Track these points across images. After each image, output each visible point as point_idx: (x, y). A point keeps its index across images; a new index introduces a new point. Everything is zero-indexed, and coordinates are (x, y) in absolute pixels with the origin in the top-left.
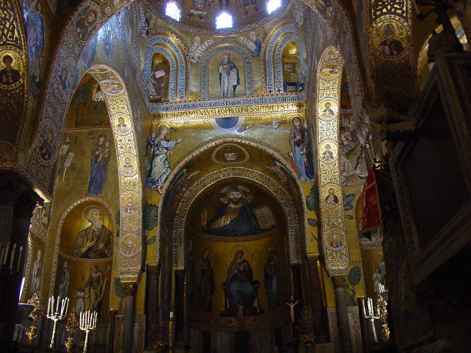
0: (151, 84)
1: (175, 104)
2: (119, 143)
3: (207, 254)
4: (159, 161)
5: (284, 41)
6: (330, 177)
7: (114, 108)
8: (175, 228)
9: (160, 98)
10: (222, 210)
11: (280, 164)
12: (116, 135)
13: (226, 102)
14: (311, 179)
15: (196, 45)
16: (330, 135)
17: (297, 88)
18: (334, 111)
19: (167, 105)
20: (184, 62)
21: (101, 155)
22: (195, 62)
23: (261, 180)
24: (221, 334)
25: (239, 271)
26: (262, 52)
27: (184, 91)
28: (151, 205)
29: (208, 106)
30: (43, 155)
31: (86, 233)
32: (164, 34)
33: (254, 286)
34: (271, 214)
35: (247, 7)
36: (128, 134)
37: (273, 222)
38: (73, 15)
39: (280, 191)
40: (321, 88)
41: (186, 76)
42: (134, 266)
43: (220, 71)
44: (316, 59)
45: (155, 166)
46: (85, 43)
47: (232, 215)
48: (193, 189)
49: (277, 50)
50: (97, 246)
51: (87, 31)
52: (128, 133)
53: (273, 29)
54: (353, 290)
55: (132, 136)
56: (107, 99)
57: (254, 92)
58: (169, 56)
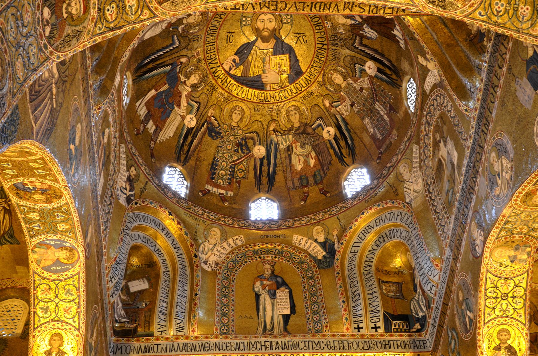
0: (119, 302)
1: (165, 342)
5: (378, 243)
7: (46, 310)
13: (271, 342)
15: (213, 241)
17: (410, 327)
20: (188, 268)
22: (209, 269)
26: (337, 259)
27: (187, 318)
29: (233, 349)
35: (306, 190)
43: (256, 290)
46: (51, 53)
49: (365, 258)
53: (359, 220)
56: (36, 285)
57: (326, 327)
58: (160, 254)
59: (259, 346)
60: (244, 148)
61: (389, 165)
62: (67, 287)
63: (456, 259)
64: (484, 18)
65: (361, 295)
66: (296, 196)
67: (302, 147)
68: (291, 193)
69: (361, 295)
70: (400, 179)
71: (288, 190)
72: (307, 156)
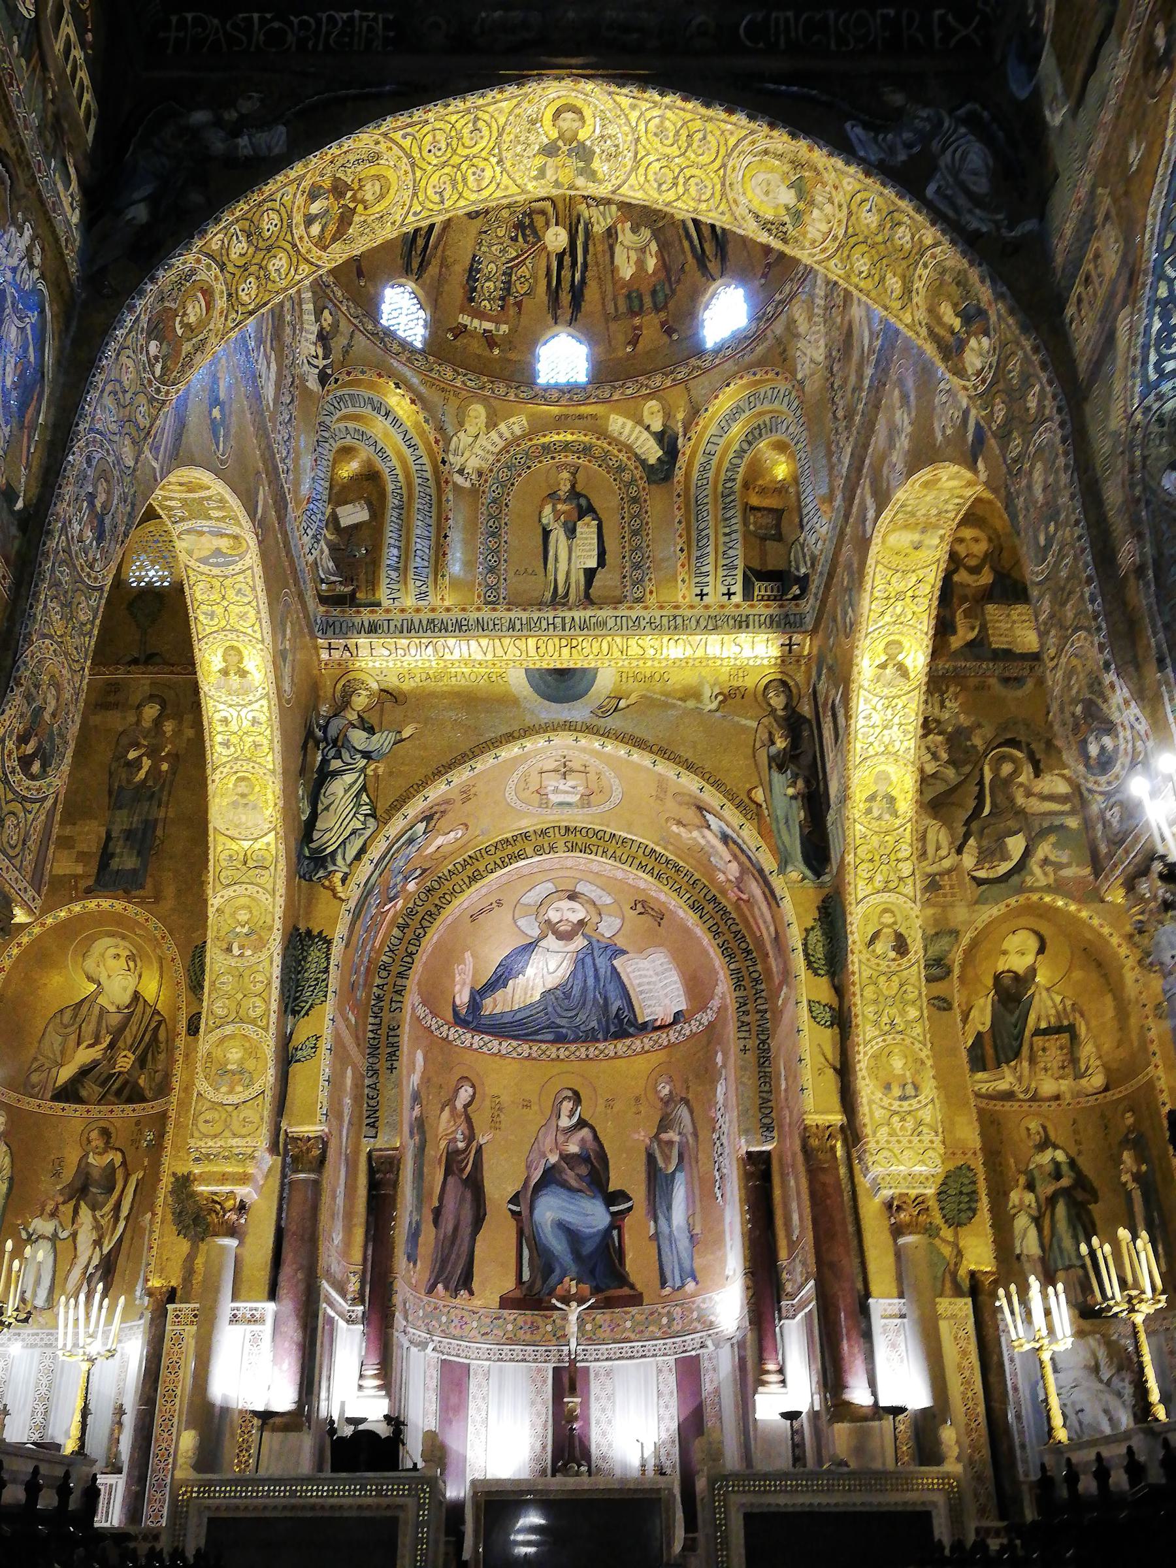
1: (400, 616)
2: (220, 729)
3: (465, 1094)
4: (340, 790)
6: (885, 873)
7: (212, 615)
8: (376, 1009)
9: (353, 593)
12: (211, 703)
13: (563, 618)
14: (818, 873)
15: (472, 430)
16: (892, 741)
17: (784, 590)
18: (910, 669)
19: (374, 617)
20: (431, 483)
21: (147, 763)
22: (467, 485)
24: (501, 1370)
25: (565, 1158)
27: (431, 577)
28: (309, 932)
30: (25, 762)
31: (75, 1016)
32: (372, 385)
33: (614, 1209)
35: (637, 321)
36: (251, 703)
38: (141, 294)
40: (876, 594)
41: (439, 528)
42: (243, 1137)
43: (544, 521)
44: (869, 501)
45: (327, 808)
46: (167, 393)
50: (112, 1061)
51: (179, 352)
52: (251, 697)
54: (955, 1245)
55: (265, 709)
59: (544, 624)
60: (528, 232)
61: (778, 297)
62: (237, 586)
63: (847, 517)
64: (841, 272)
65: (712, 538)
66: (619, 331)
67: (635, 230)
68: (613, 326)
69: (712, 538)
70: (791, 331)
71: (607, 321)
72: (643, 250)
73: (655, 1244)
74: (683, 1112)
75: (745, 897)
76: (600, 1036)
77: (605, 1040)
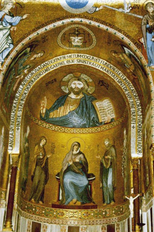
8: (13, 110)
10: (62, 100)
11: (129, 51)
23: (106, 69)
24: (51, 226)
25: (75, 163)
34: (112, 107)
37: (113, 116)
39: (125, 81)
47: (72, 106)
48: (35, 72)
73: (102, 189)
74: (113, 150)
75: (136, 77)
76: (87, 126)
77: (89, 127)
